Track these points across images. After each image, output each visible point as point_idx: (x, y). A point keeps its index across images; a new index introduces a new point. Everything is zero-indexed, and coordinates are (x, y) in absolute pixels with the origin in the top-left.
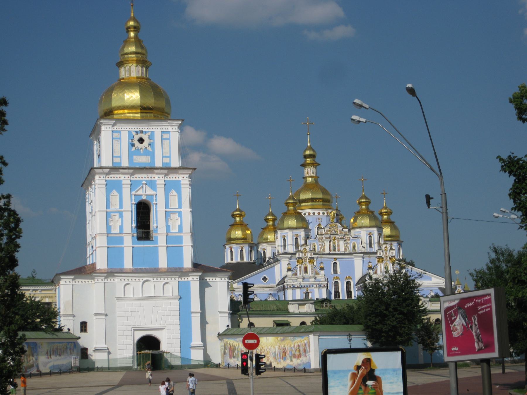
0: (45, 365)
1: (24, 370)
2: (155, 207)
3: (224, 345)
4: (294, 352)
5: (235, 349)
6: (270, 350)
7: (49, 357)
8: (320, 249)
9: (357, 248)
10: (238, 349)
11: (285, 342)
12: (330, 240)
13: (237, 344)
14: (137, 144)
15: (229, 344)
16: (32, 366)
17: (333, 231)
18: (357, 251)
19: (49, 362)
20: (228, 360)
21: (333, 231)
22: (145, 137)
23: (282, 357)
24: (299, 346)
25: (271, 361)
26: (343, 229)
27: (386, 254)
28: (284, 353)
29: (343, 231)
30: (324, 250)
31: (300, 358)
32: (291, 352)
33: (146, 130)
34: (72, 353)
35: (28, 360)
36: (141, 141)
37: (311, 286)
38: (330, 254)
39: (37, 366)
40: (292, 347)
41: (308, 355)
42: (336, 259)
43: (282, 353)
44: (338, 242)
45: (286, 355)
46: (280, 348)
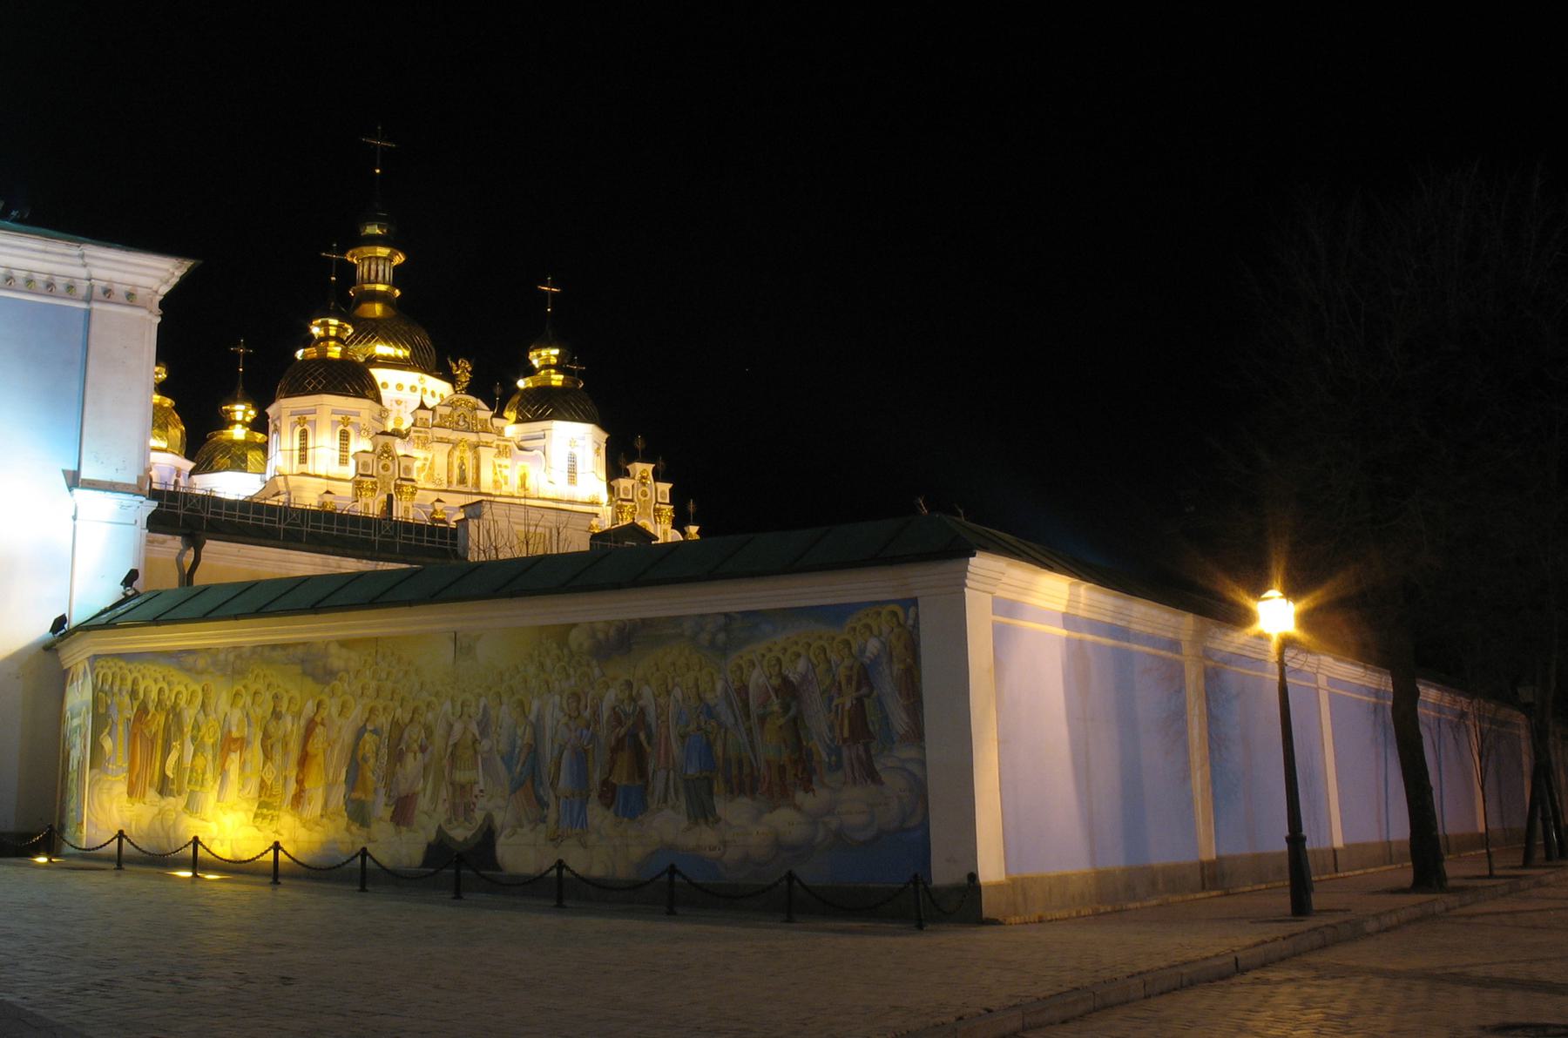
3: (96, 701)
5: (172, 728)
6: (481, 734)
10: (204, 730)
13: (193, 693)
15: (133, 694)
17: (461, 423)
21: (461, 423)
23: (605, 783)
24: (789, 691)
25: (489, 818)
26: (494, 419)
27: (646, 496)
31: (800, 796)
40: (709, 696)
45: (651, 767)
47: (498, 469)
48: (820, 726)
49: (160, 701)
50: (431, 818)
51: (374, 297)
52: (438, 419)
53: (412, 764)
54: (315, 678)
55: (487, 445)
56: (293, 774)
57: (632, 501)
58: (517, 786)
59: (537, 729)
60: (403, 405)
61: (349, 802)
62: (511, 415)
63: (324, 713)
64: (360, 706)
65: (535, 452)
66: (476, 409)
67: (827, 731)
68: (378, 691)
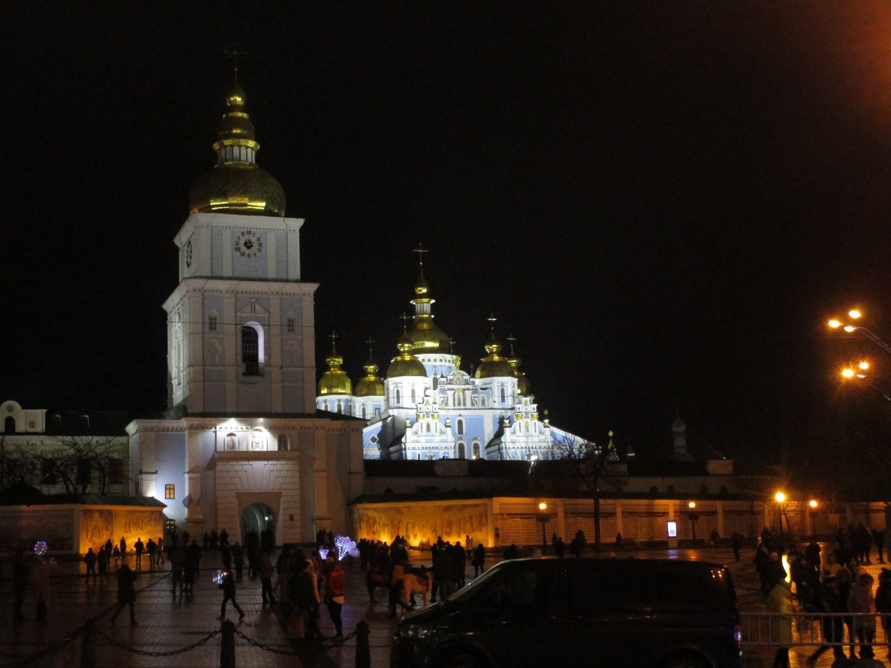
3: (359, 517)
7: (128, 530)
8: (442, 404)
9: (486, 403)
12: (454, 391)
14: (244, 249)
15: (367, 516)
17: (458, 381)
18: (487, 407)
21: (458, 381)
22: (254, 240)
27: (527, 410)
30: (447, 404)
33: (255, 230)
34: (157, 524)
36: (248, 245)
37: (435, 448)
38: (453, 409)
42: (460, 415)
44: (464, 394)
47: (473, 398)
51: (423, 320)
52: (448, 381)
55: (468, 389)
56: (396, 530)
57: (521, 412)
58: (433, 532)
60: (437, 367)
62: (478, 373)
65: (488, 390)
66: (463, 376)
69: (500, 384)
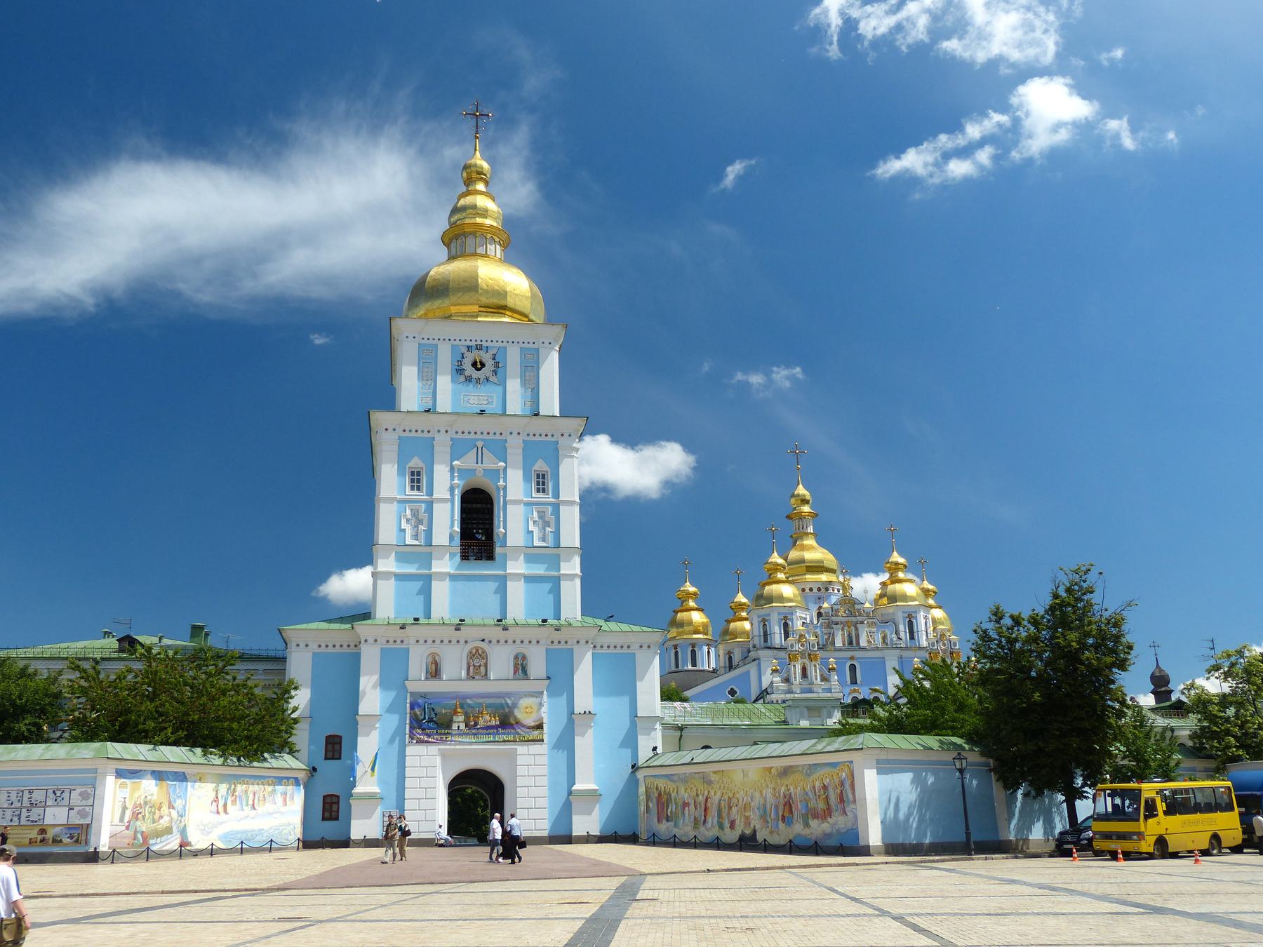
0: (205, 831)
1: (141, 841)
2: (502, 494)
4: (812, 804)
7: (221, 810)
11: (789, 780)
13: (674, 789)
14: (470, 370)
15: (657, 788)
16: (168, 831)
19: (221, 823)
20: (654, 827)
21: (847, 612)
23: (783, 815)
24: (825, 788)
25: (754, 827)
28: (787, 807)
29: (864, 611)
30: (833, 643)
31: (829, 818)
32: (806, 801)
33: (489, 344)
34: (288, 802)
35: (156, 817)
39: (183, 832)
40: (806, 789)
41: (849, 809)
42: (852, 658)
43: (781, 807)
46: (777, 794)
48: (833, 799)
49: (665, 791)
50: (740, 828)
53: (734, 810)
54: (707, 783)
55: (862, 623)
59: (765, 799)
61: (718, 822)
63: (710, 794)
64: (719, 794)
67: (834, 799)
68: (724, 787)
69: (907, 615)
